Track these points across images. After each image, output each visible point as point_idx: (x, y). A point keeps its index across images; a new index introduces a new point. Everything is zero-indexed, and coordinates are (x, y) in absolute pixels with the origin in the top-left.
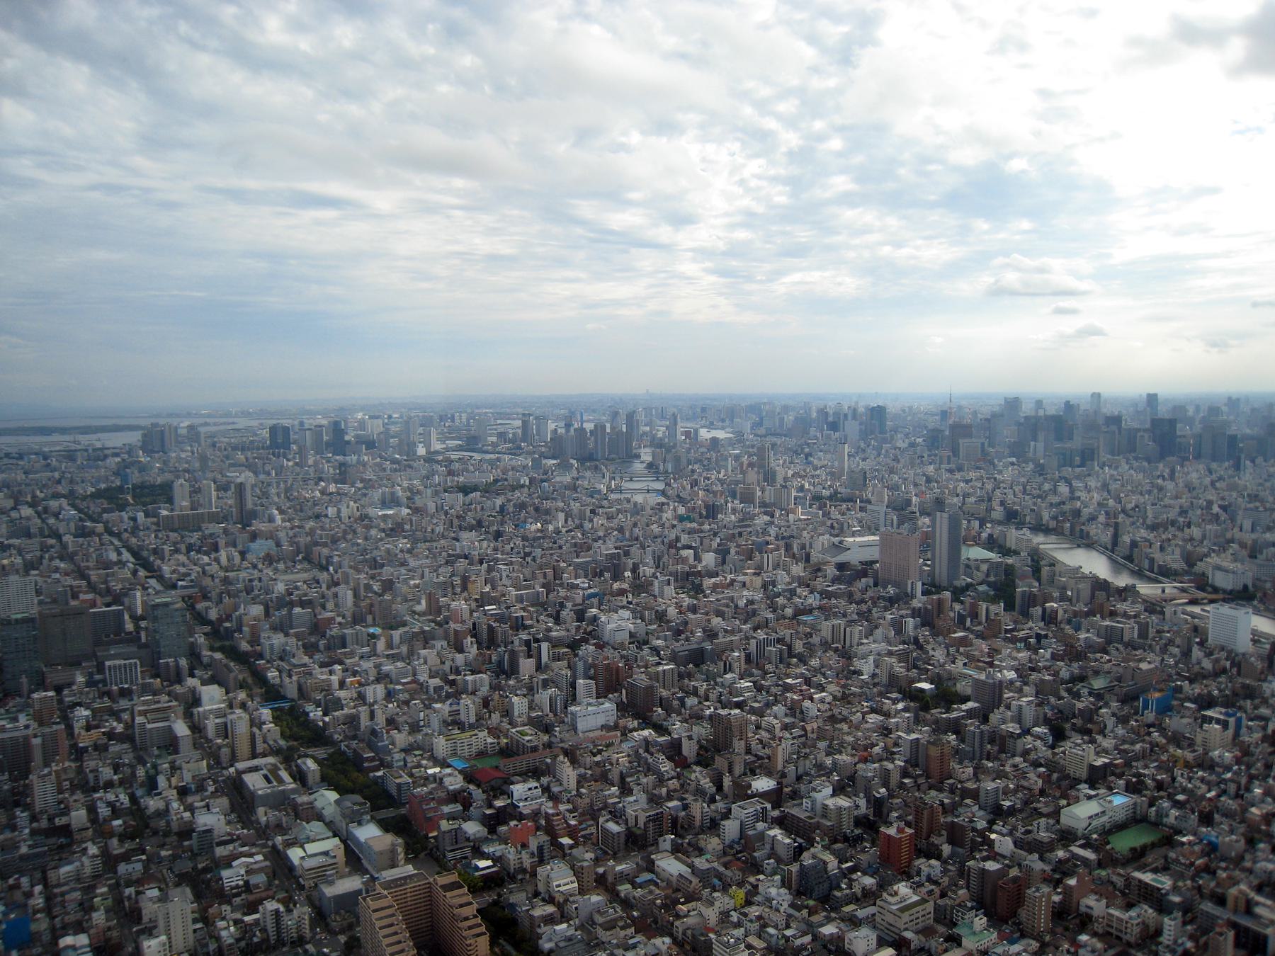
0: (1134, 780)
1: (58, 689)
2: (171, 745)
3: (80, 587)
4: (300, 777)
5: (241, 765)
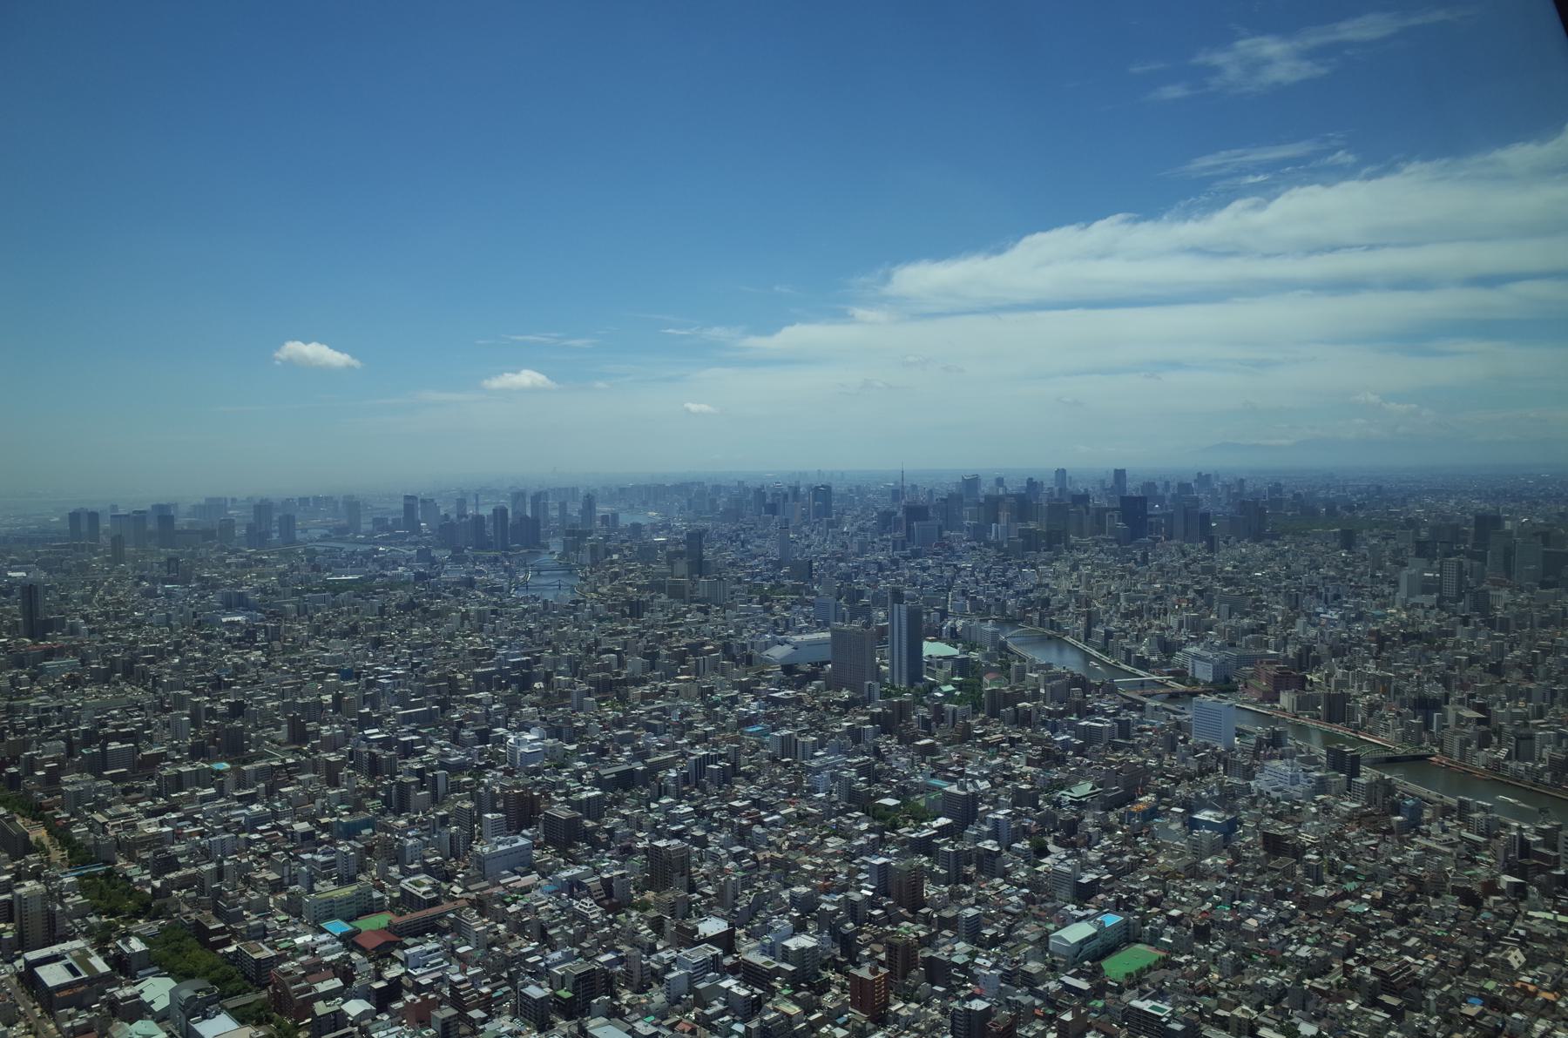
0: (1124, 896)
5: (32, 955)
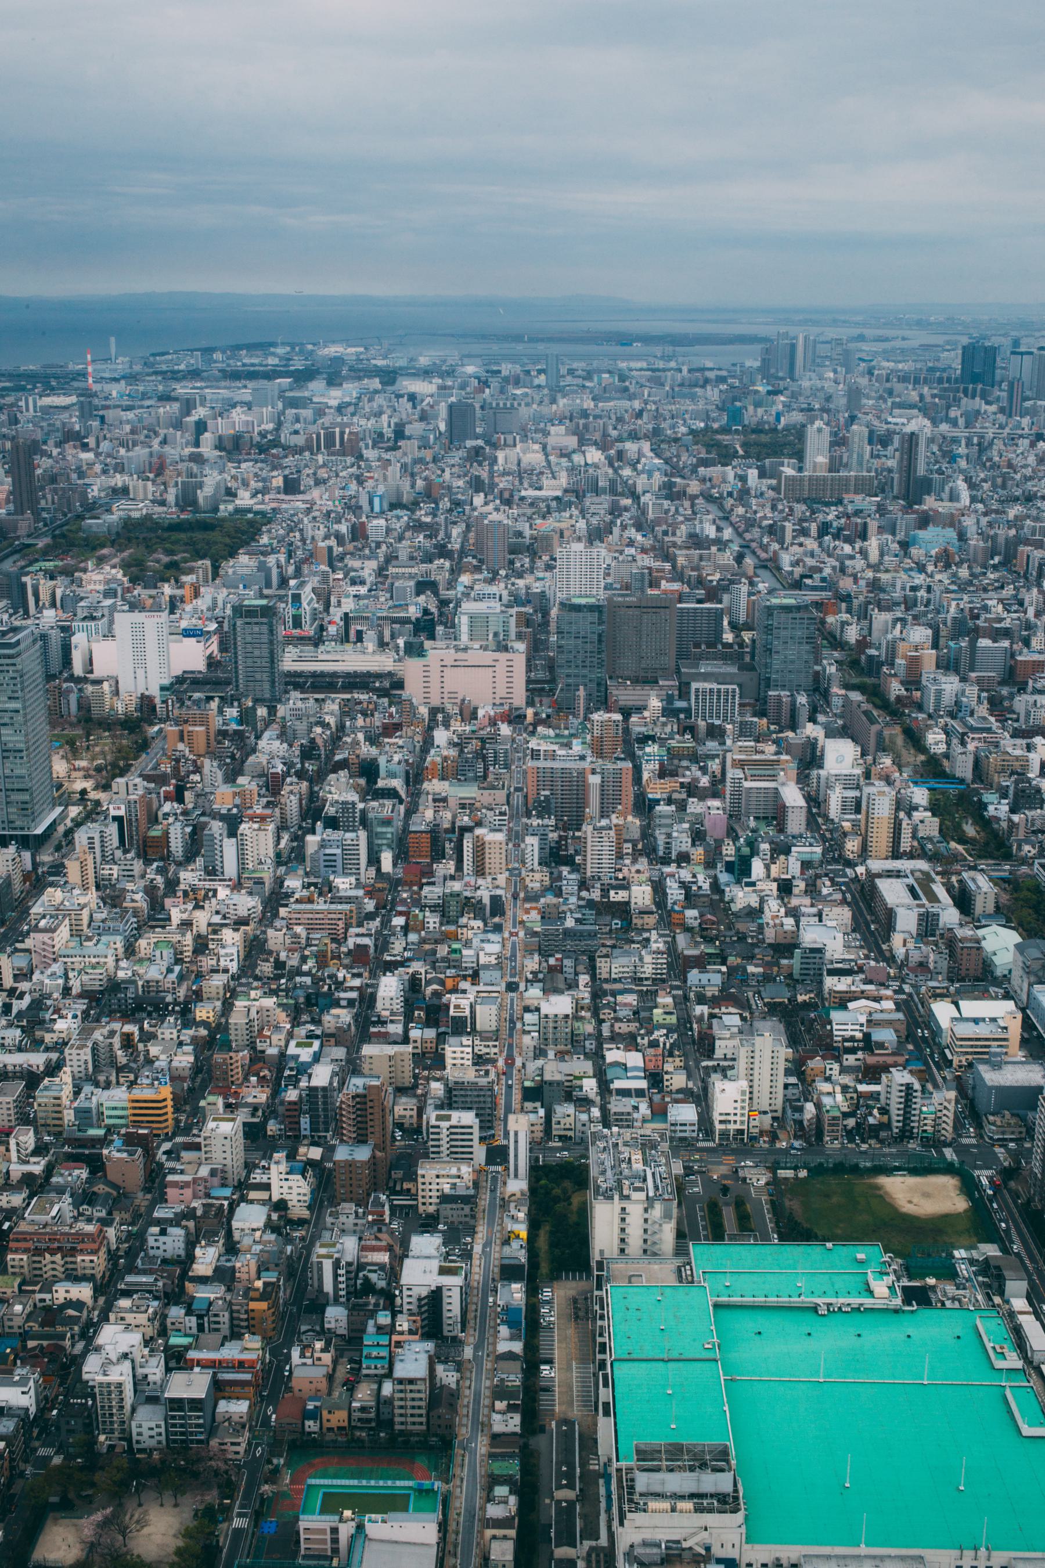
1: (626, 713)
2: (774, 818)
3: (663, 571)
4: (963, 900)
5: (876, 865)
